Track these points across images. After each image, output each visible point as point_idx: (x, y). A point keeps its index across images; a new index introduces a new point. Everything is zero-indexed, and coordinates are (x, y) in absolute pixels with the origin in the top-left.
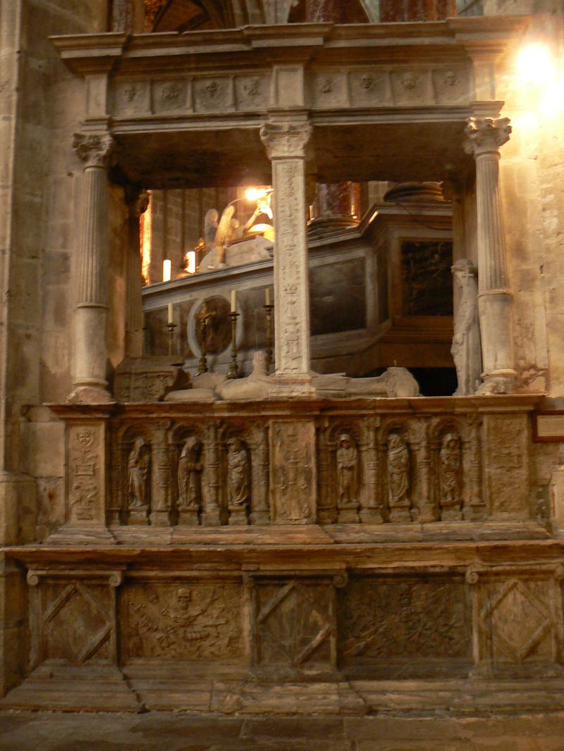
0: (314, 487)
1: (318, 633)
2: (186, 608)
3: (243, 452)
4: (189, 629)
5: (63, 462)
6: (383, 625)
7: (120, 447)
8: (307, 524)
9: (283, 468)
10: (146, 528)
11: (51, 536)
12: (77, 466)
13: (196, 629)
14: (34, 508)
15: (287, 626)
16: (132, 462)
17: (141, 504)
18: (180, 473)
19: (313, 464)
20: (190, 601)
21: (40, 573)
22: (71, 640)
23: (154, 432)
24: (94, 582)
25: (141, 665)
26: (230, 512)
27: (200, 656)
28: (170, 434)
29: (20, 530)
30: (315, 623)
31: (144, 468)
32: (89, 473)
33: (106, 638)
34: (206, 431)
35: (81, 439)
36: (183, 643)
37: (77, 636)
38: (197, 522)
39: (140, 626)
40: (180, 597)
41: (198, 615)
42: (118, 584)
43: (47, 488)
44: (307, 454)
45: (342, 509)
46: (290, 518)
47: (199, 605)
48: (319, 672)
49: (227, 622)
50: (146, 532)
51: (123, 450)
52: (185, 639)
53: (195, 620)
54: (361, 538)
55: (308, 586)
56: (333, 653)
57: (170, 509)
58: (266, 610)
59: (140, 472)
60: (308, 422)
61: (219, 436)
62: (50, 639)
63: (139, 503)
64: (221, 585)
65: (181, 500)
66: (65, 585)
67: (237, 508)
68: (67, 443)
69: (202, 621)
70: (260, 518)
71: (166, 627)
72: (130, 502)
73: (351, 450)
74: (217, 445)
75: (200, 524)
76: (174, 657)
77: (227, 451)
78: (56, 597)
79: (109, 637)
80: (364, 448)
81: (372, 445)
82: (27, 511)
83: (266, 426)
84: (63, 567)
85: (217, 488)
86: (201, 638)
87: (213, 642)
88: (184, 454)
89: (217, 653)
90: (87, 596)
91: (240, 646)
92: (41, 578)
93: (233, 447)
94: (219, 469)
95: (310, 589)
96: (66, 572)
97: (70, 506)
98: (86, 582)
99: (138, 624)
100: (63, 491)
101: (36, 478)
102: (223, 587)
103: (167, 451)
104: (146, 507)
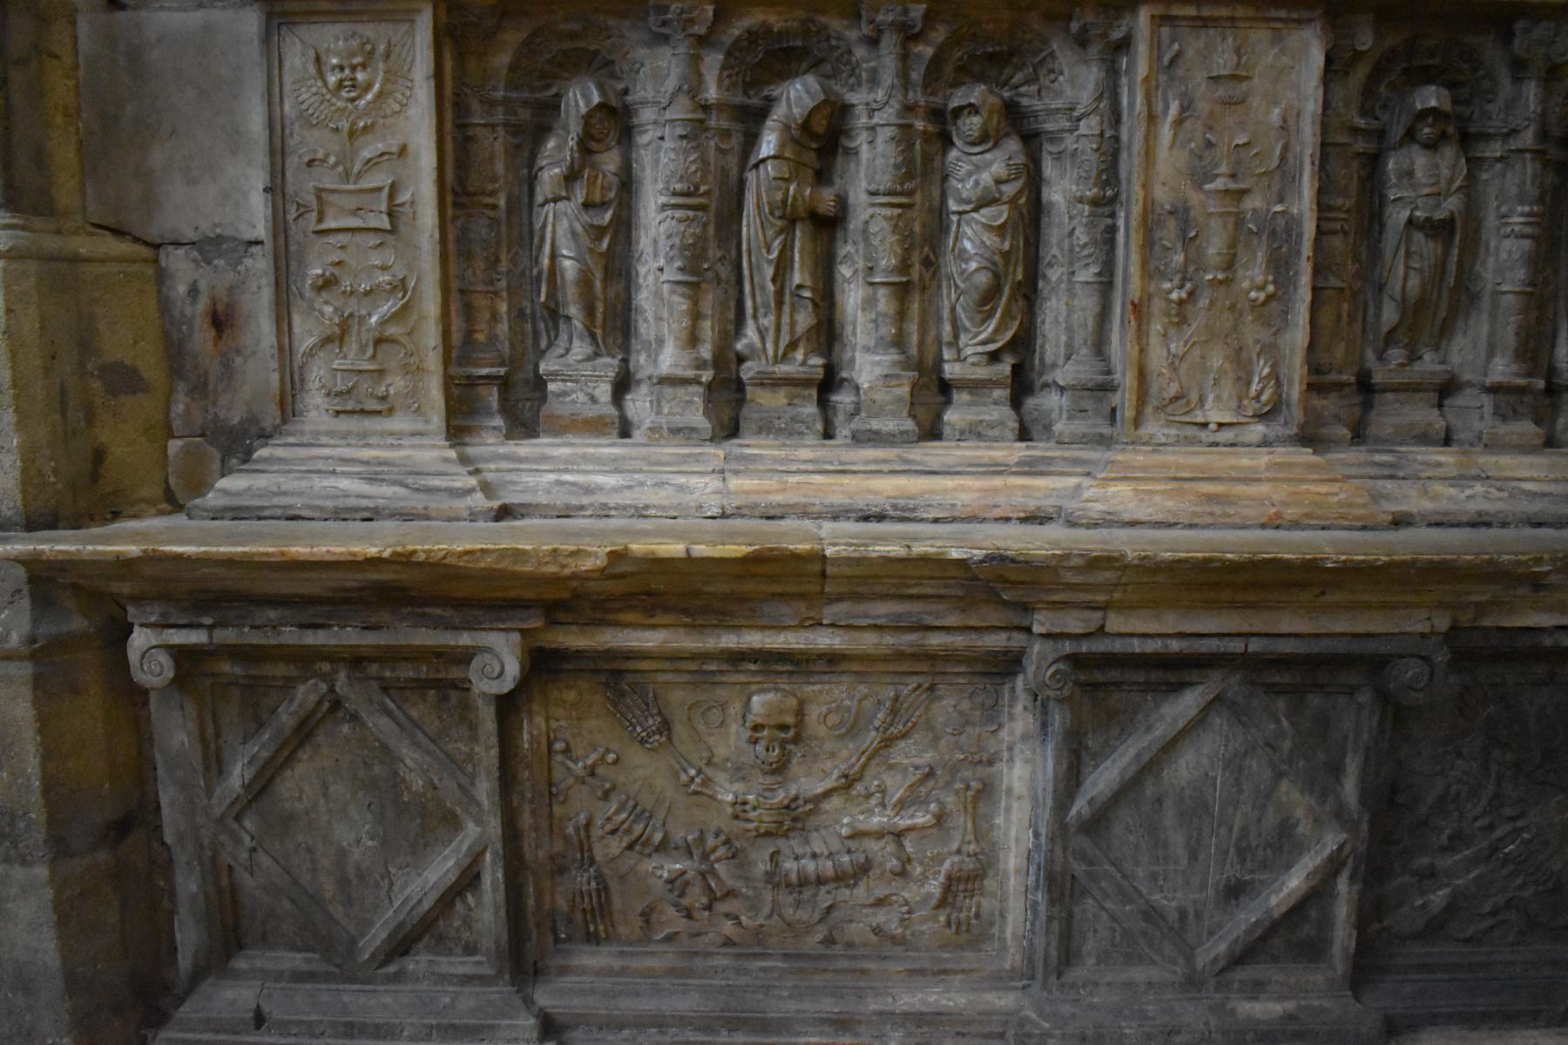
0: (1304, 295)
1: (1288, 867)
2: (780, 768)
3: (1013, 145)
4: (795, 844)
5: (258, 179)
6: (1522, 830)
7: (500, 117)
8: (1265, 443)
9: (1181, 212)
10: (609, 448)
11: (222, 483)
12: (319, 192)
13: (818, 846)
14: (149, 364)
15: (1178, 840)
16: (550, 176)
17: (589, 350)
18: (750, 226)
19: (1304, 203)
20: (797, 740)
21: (178, 637)
22: (329, 888)
23: (642, 52)
24: (407, 672)
26: (946, 388)
27: (829, 941)
28: (713, 62)
29: (99, 456)
30: (1285, 828)
31: (604, 205)
32: (373, 223)
33: (469, 879)
34: (860, 52)
35: (332, 79)
37: (351, 872)
38: (819, 426)
39: (596, 833)
40: (757, 728)
41: (827, 794)
42: (507, 685)
43: (203, 285)
44: (1283, 158)
45: (1386, 389)
46: (1200, 419)
47: (833, 755)
48: (1290, 1006)
49: (940, 818)
50: (615, 465)
51: (515, 129)
52: (775, 879)
54: (1485, 506)
55: (1274, 690)
56: (1342, 935)
57: (707, 376)
58: (1103, 779)
59: (586, 218)
60: (1299, 22)
61: (916, 76)
62: (246, 881)
63: (580, 349)
64: (926, 681)
65: (751, 332)
66: (288, 685)
67: (982, 373)
68: (273, 98)
69: (845, 817)
70: (1078, 412)
71: (701, 838)
72: (543, 343)
73: (1449, 152)
74: (909, 109)
75: (828, 434)
76: (728, 942)
77: (946, 141)
78: (261, 725)
79: (478, 876)
80: (1495, 149)
81: (1528, 138)
82: (124, 380)
83: (1117, 35)
84: (272, 614)
85: (902, 291)
86: (840, 878)
87: (881, 892)
88: (768, 145)
89: (894, 928)
90: (380, 725)
91: (987, 904)
92: (182, 655)
93: (973, 123)
94: (914, 213)
95: (1281, 704)
96: (290, 636)
97: (298, 359)
98: (373, 669)
100: (267, 294)
101: (157, 247)
102: (932, 688)
103: (695, 132)
104: (609, 365)
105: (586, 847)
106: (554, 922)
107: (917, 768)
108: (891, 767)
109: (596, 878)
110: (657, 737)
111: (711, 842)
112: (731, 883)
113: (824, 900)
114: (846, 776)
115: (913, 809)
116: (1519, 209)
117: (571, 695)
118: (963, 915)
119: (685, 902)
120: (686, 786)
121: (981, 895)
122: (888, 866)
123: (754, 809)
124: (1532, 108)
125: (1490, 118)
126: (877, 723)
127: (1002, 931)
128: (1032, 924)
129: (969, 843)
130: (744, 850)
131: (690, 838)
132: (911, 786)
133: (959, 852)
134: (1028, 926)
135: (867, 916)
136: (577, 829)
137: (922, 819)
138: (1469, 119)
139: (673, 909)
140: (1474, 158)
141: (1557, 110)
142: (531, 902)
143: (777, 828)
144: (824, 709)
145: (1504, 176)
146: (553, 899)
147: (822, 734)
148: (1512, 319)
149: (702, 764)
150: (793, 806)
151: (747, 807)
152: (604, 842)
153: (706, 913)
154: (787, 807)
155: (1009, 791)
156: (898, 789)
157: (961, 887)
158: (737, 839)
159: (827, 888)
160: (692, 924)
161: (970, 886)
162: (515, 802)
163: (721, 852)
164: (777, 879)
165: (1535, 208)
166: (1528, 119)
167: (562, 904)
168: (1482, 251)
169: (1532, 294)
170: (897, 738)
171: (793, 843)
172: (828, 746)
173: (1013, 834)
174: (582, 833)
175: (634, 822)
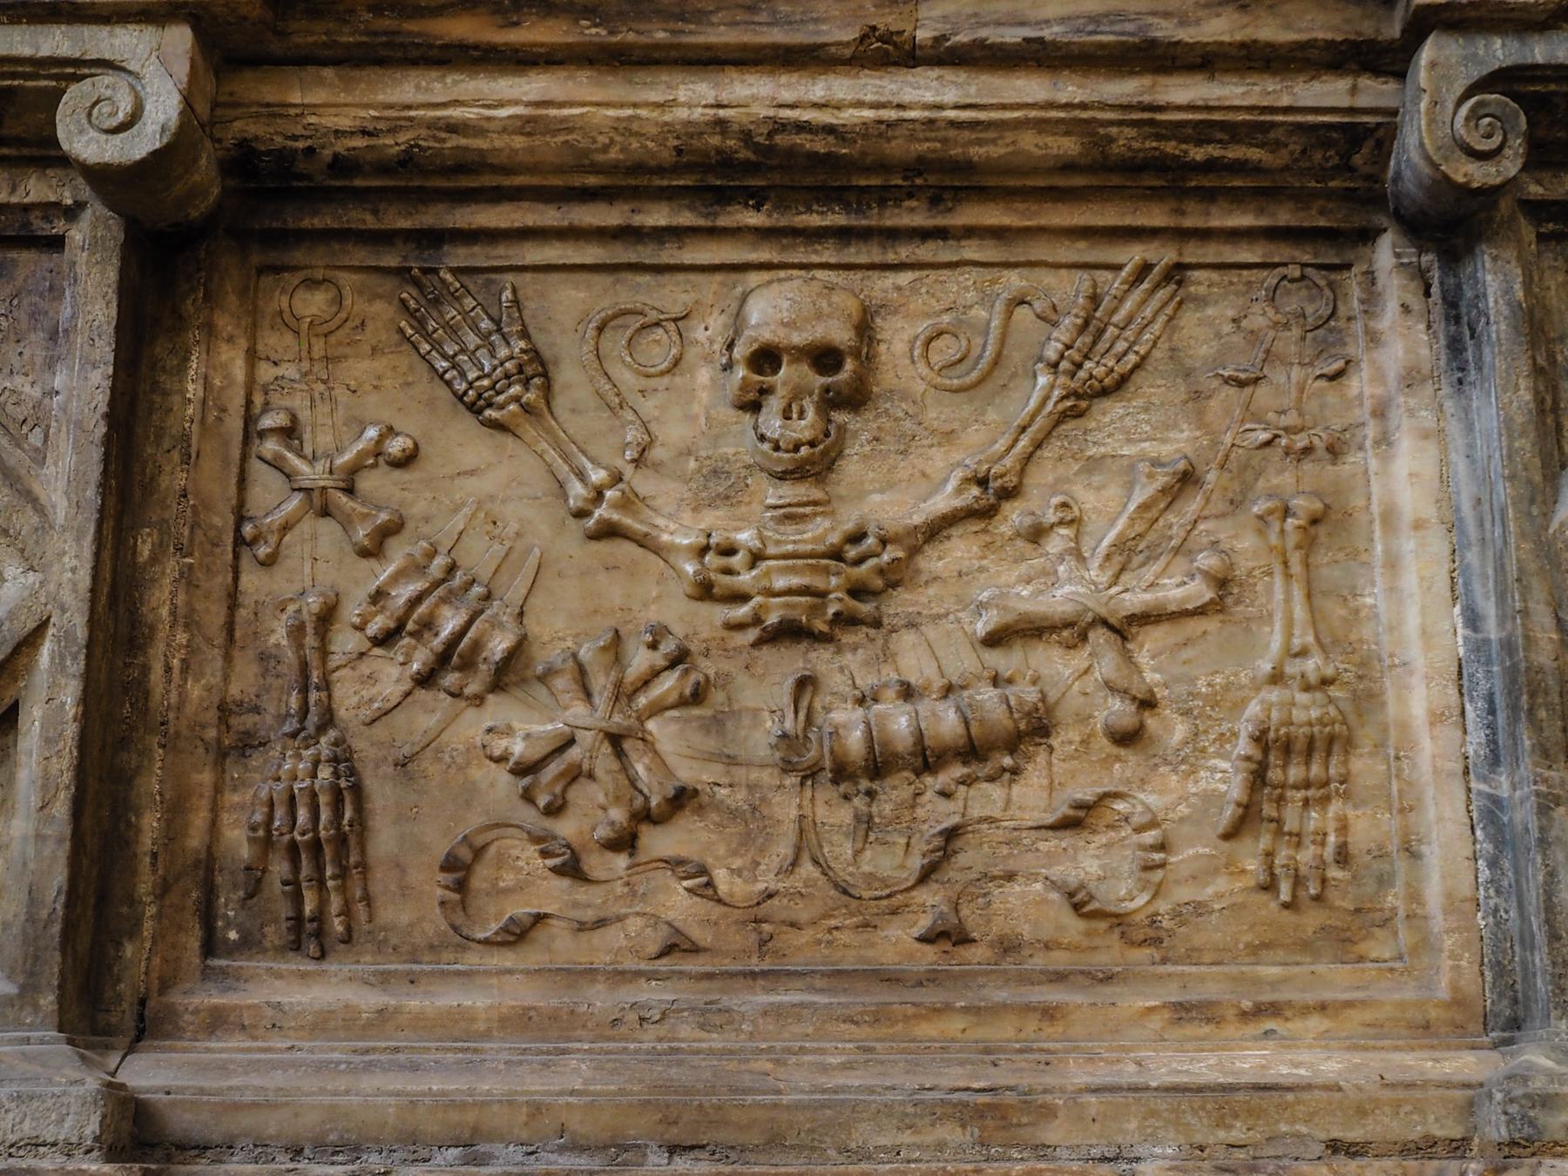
20: (855, 398)
25: (321, 1024)
27: (948, 935)
36: (786, 807)
39: (345, 642)
41: (936, 530)
47: (948, 437)
53: (894, 578)
64: (1163, 255)
71: (615, 646)
76: (677, 946)
86: (972, 751)
99: (327, 618)
102: (1177, 273)
105: (315, 678)
106: (210, 892)
107: (1156, 463)
108: (1093, 465)
109: (335, 760)
110: (516, 389)
111: (640, 660)
112: (687, 773)
113: (937, 814)
114: (983, 482)
115: (1156, 567)
117: (313, 304)
118: (1306, 856)
119: (566, 828)
120: (581, 514)
121: (1346, 796)
122: (1100, 719)
123: (756, 558)
126: (1051, 353)
127: (1415, 896)
128: (1493, 864)
129: (1303, 653)
130: (725, 680)
131: (585, 654)
132: (1144, 507)
133: (1277, 678)
134: (1485, 874)
135: (1051, 858)
136: (297, 631)
137: (1180, 589)
139: (532, 850)
142: (150, 824)
143: (815, 610)
144: (922, 327)
146: (214, 826)
147: (920, 387)
149: (623, 464)
150: (852, 552)
151: (737, 561)
152: (365, 668)
153: (621, 861)
154: (836, 554)
155: (1389, 518)
156: (1113, 522)
157: (1295, 773)
158: (707, 654)
159: (944, 779)
160: (582, 894)
161: (1316, 770)
162: (145, 551)
163: (668, 684)
164: (812, 754)
167: (237, 841)
170: (1105, 392)
171: (848, 658)
172: (935, 415)
173: (1413, 621)
174: (310, 640)
175: (444, 600)
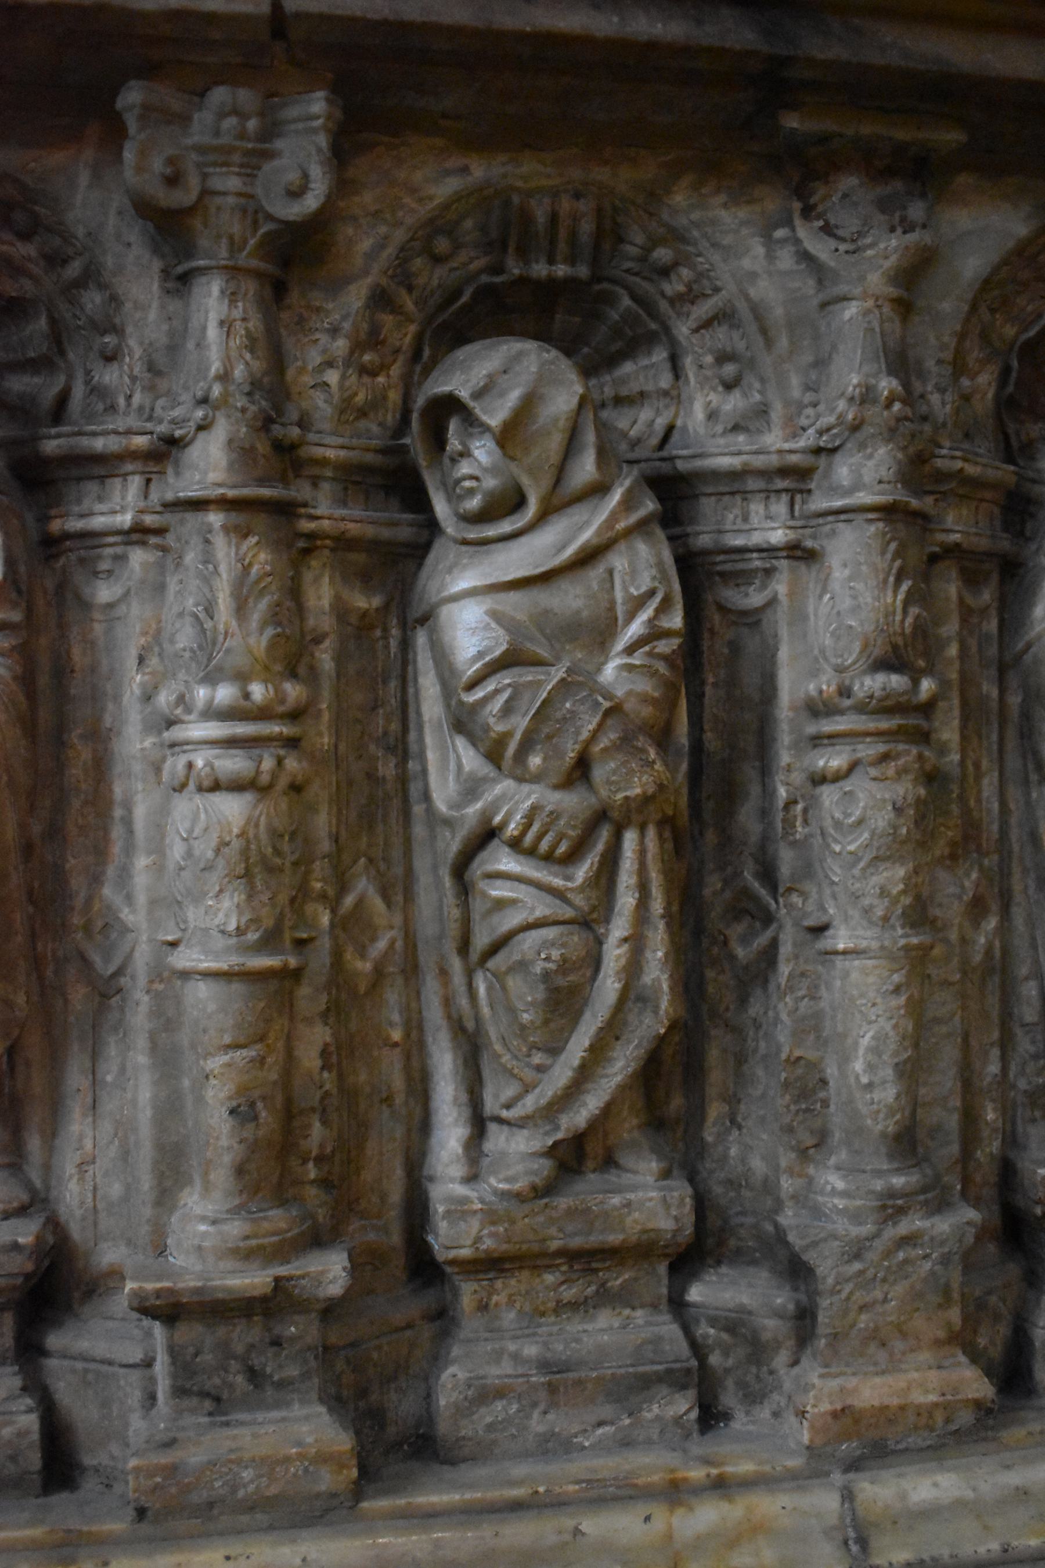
116: (202, 693)
124: (215, 367)
125: (112, 408)
138: (59, 411)
140: (67, 536)
141: (332, 377)
145: (160, 588)
148: (216, 1063)
165: (258, 691)
166: (204, 401)
168: (117, 832)
169: (294, 975)
